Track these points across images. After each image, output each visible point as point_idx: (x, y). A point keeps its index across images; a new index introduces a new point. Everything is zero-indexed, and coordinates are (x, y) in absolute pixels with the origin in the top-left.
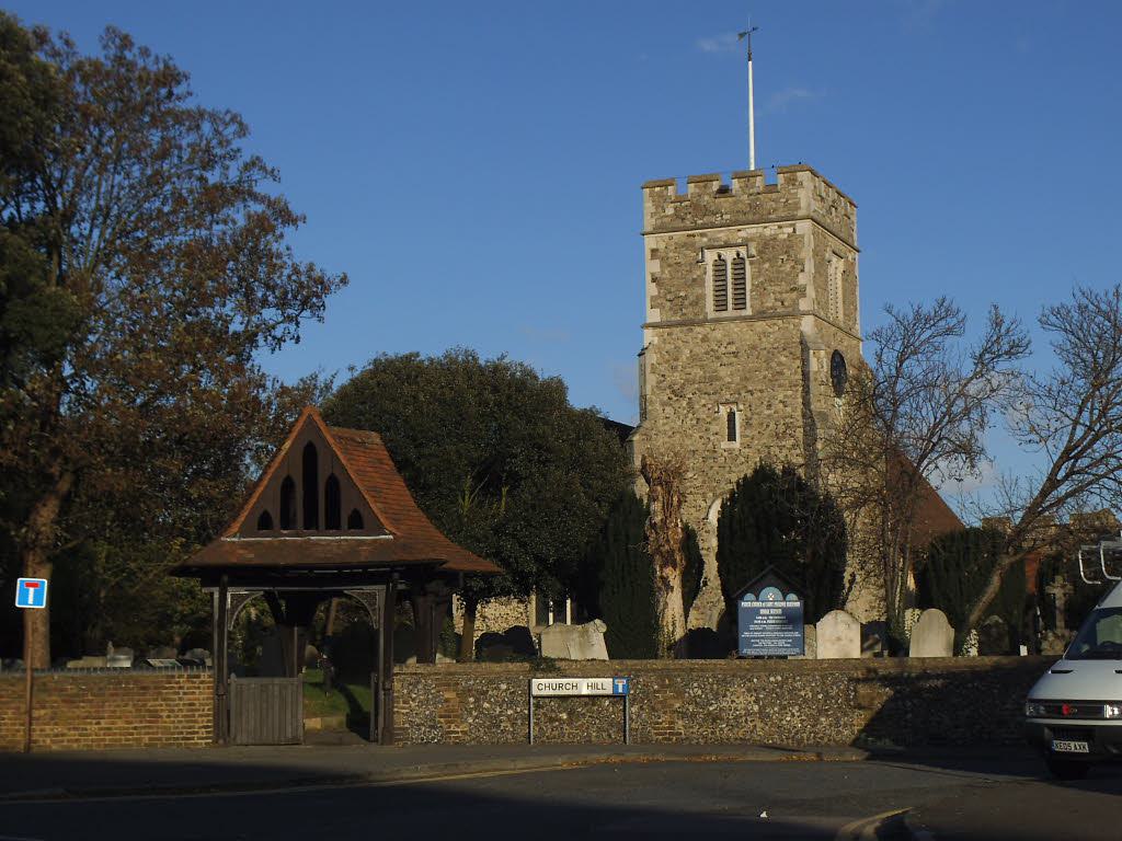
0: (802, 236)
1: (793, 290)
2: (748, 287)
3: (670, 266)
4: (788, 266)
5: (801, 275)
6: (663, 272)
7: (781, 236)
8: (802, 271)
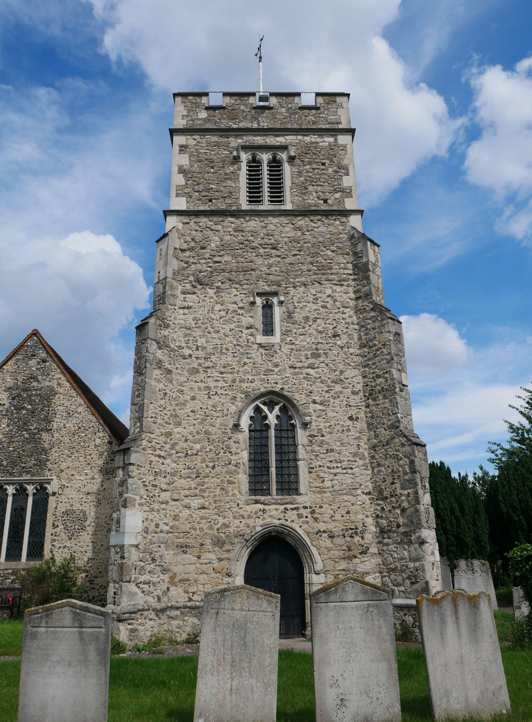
0: (345, 146)
1: (336, 191)
2: (287, 183)
3: (200, 161)
4: (330, 170)
5: (345, 178)
6: (192, 166)
7: (321, 144)
8: (347, 174)
